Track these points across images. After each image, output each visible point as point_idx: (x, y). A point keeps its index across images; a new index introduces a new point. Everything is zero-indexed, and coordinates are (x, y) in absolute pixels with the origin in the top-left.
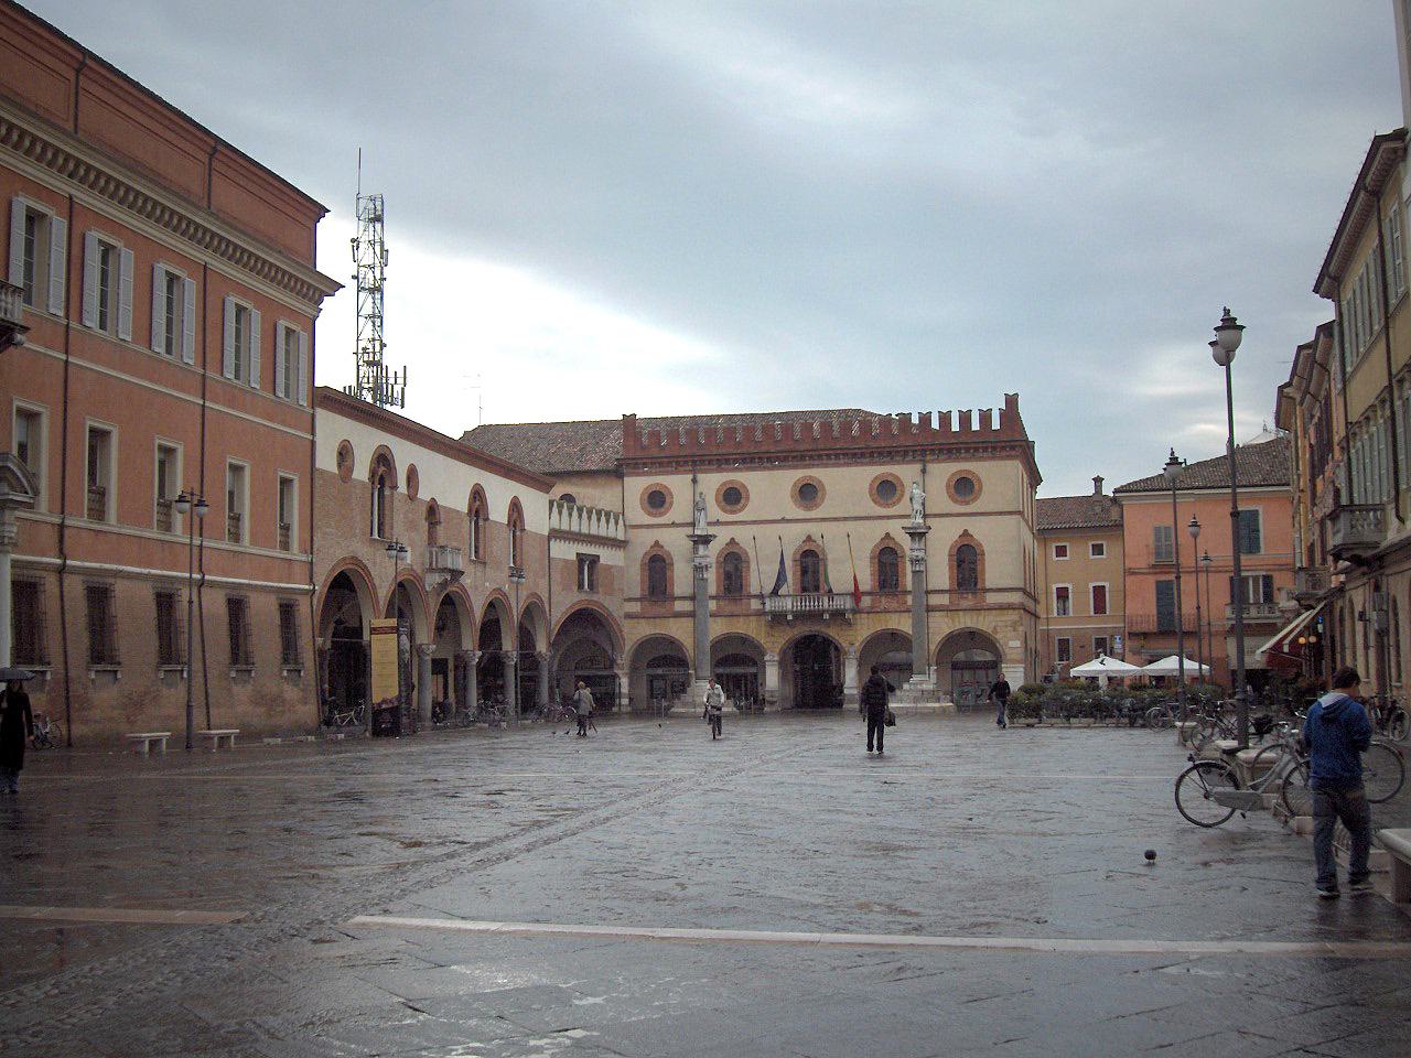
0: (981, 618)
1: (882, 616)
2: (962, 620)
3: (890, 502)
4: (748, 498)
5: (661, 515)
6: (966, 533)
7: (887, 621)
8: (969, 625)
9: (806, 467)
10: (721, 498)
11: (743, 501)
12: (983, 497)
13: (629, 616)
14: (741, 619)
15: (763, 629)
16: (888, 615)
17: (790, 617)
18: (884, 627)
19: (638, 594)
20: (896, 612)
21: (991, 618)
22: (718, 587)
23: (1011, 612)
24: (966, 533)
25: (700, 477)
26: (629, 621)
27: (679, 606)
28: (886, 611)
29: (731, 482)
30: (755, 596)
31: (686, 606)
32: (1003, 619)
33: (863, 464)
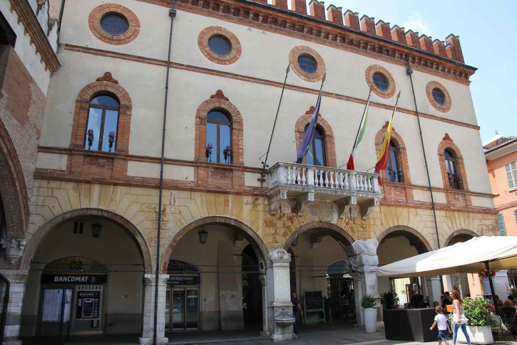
0: (471, 220)
1: (393, 208)
2: (458, 222)
3: (386, 93)
4: (239, 51)
5: (119, 42)
6: (447, 137)
7: (398, 218)
8: (464, 227)
9: (304, 38)
10: (205, 42)
11: (234, 52)
12: (450, 111)
13: (41, 175)
14: (231, 197)
15: (261, 215)
16: (399, 209)
17: (311, 197)
18: (396, 224)
19: (66, 144)
20: (406, 206)
21: (477, 222)
22: (198, 150)
23: (489, 216)
24: (447, 137)
25: (180, 13)
26: (44, 183)
27: (135, 170)
28: (398, 204)
29: (219, 28)
30: (253, 170)
31: (150, 171)
32: (487, 222)
33: (357, 52)
